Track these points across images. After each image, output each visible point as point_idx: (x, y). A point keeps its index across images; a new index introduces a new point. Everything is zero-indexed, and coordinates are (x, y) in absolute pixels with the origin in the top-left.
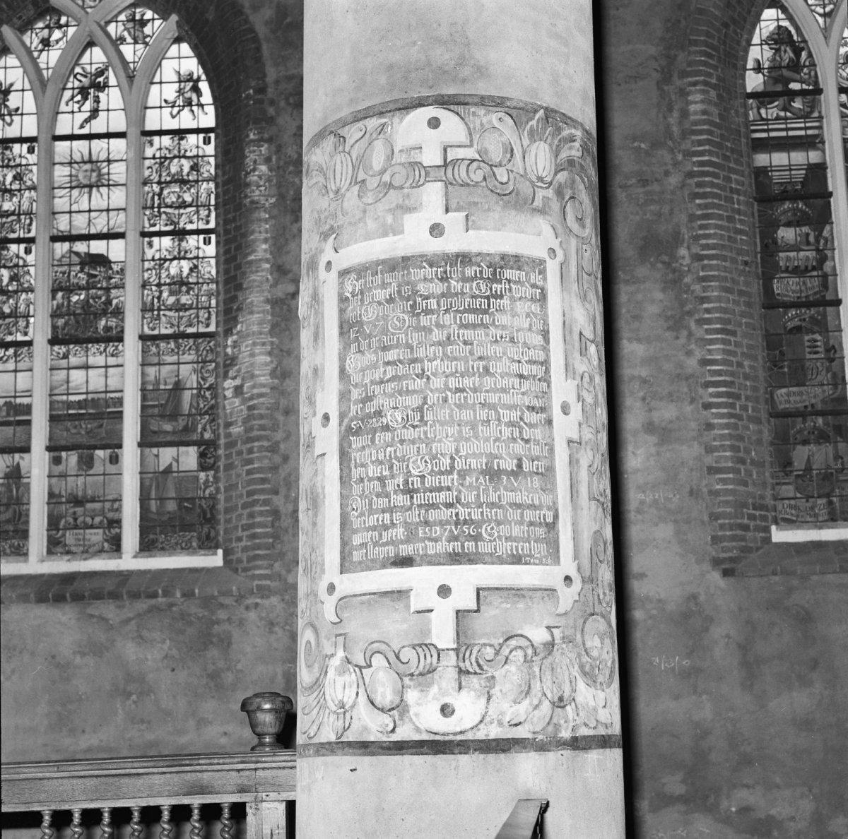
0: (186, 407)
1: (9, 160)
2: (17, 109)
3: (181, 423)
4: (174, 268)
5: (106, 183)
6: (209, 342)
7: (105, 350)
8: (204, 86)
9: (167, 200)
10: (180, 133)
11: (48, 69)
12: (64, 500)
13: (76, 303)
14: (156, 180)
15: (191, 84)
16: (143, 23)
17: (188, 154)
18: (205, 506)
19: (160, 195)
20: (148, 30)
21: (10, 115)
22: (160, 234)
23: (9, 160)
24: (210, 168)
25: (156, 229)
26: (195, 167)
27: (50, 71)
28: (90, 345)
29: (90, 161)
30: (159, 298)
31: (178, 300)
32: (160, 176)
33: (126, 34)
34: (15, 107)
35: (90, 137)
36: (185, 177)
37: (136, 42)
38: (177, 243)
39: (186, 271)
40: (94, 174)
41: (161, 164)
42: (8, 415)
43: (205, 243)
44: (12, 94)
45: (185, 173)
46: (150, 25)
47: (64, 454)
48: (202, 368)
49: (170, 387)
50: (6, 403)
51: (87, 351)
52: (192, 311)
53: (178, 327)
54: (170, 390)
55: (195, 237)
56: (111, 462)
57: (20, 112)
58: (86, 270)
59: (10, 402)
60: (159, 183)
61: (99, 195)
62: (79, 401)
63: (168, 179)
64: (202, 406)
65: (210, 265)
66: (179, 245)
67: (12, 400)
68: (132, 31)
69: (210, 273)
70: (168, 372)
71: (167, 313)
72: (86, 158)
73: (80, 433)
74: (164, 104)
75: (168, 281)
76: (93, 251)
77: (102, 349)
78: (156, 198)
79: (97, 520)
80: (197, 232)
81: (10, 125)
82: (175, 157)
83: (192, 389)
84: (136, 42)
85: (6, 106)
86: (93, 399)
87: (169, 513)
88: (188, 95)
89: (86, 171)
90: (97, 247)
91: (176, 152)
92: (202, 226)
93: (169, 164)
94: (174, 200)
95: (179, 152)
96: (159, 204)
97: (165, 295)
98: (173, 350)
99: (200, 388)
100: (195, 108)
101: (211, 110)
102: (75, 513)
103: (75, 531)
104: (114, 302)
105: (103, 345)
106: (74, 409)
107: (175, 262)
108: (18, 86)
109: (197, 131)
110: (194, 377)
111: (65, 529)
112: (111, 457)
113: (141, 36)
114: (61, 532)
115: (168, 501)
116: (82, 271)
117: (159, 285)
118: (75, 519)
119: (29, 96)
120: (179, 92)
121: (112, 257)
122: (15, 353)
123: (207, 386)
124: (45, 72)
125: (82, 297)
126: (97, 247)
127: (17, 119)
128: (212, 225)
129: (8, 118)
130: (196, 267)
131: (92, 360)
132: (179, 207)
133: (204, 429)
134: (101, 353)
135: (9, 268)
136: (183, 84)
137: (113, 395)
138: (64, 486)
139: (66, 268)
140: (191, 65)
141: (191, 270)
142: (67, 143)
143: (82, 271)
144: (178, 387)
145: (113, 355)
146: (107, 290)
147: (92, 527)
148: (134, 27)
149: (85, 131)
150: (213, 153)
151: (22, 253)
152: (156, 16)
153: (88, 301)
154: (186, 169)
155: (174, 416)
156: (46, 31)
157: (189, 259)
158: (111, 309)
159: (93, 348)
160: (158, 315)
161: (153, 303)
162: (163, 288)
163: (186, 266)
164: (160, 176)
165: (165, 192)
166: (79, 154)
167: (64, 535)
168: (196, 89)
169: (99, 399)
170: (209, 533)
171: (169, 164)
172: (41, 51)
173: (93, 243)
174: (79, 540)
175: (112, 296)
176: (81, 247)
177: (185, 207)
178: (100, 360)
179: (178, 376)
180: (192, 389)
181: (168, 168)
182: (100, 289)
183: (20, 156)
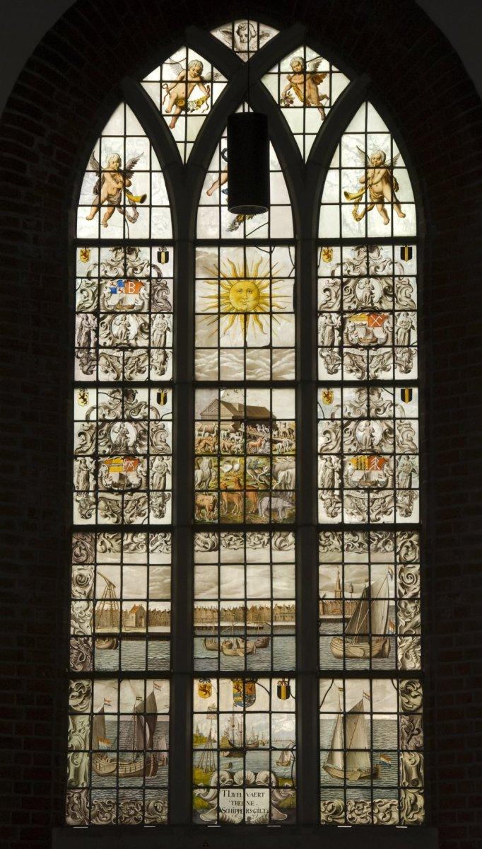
0: (380, 626)
1: (135, 269)
2: (144, 198)
3: (377, 647)
4: (362, 431)
5: (268, 309)
6: (410, 536)
7: (270, 540)
8: (402, 176)
9: (352, 337)
10: (369, 244)
11: (186, 142)
12: (215, 746)
13: (228, 474)
14: (336, 308)
15: (383, 171)
16: (316, 78)
17: (380, 272)
18: (409, 763)
19: (341, 329)
20: (323, 88)
21: (134, 206)
22: (342, 384)
23: (135, 269)
24: (409, 294)
25: (337, 377)
26: (390, 292)
27: (190, 146)
28: (248, 534)
29: (246, 278)
30: (341, 472)
31: (367, 476)
32: (342, 302)
33: (292, 91)
34: (140, 195)
35: (245, 243)
36: (377, 305)
37: (306, 105)
38: (365, 397)
39: (378, 436)
40: (251, 296)
41: (343, 284)
42: (138, 625)
43: (403, 399)
44: (135, 174)
45: (376, 299)
46: (326, 80)
47: (214, 682)
48: (402, 570)
49: (357, 595)
50: (135, 607)
51: (245, 541)
52: (386, 493)
53: (369, 514)
54: (360, 600)
55: (391, 390)
56: (279, 696)
57: (147, 202)
58: (242, 429)
59: (141, 608)
60: (341, 312)
61: (257, 325)
62: (235, 610)
63: (354, 307)
64: (402, 622)
65: (411, 430)
66: (368, 399)
67: (144, 604)
68: (301, 87)
69: (411, 440)
70: (355, 576)
71: (353, 493)
72: (240, 273)
73: (236, 655)
74: (344, 200)
75: (354, 449)
76: (251, 402)
77: (266, 539)
78: (337, 333)
79: (263, 775)
80: (393, 383)
81: (134, 220)
82: (361, 276)
83: (389, 599)
84: (306, 105)
85: (126, 191)
86: (254, 609)
87: (359, 770)
88: (378, 188)
89: (240, 291)
90: (258, 398)
91: (363, 270)
92: (400, 376)
93: (354, 286)
94: (362, 335)
95: (368, 269)
96: (342, 342)
97: (349, 468)
98: (361, 544)
99: (398, 599)
100: (388, 207)
101: (410, 211)
102: (231, 765)
103: (232, 791)
104: (281, 475)
105: (267, 534)
106: (228, 620)
107: (363, 423)
108: (142, 165)
109: (392, 241)
110: (392, 584)
111: (218, 787)
112: (279, 688)
113: (314, 97)
114: (212, 792)
115: (359, 755)
116: (236, 430)
117: (341, 455)
118: (232, 775)
119: (159, 179)
120: (366, 182)
121: (277, 413)
122: (148, 540)
123: (409, 595)
124: (181, 147)
125: (237, 466)
126: (258, 398)
127: (144, 212)
128: (413, 375)
129: (130, 211)
130: (392, 431)
131: (252, 555)
132: (368, 348)
133: (407, 656)
134: (264, 545)
135: (137, 421)
136: (370, 171)
137: (281, 603)
138: (214, 728)
139: (213, 425)
140: (382, 143)
141: (385, 434)
142: (214, 250)
143: (236, 430)
144: (369, 597)
145: (280, 549)
146: (270, 457)
147: (255, 786)
148: (304, 83)
149: (238, 234)
150: (414, 272)
151: (154, 402)
152: (334, 69)
153: (245, 473)
154: (378, 293)
155: (367, 636)
156: (182, 86)
157: (381, 419)
158: (275, 485)
159: (253, 538)
160: (341, 496)
161: (333, 480)
162: (347, 458)
163: (378, 428)
164: (342, 302)
165: (349, 325)
166: (230, 267)
167: (217, 796)
168: (390, 180)
169: (261, 608)
170: (416, 800)
171: (354, 286)
172: (177, 116)
173: (251, 393)
174: (237, 803)
175: (277, 468)
176: (234, 397)
177: (377, 347)
178: (261, 554)
179: (369, 580)
180: (389, 599)
181: (353, 291)
182: (262, 455)
183: (151, 265)
